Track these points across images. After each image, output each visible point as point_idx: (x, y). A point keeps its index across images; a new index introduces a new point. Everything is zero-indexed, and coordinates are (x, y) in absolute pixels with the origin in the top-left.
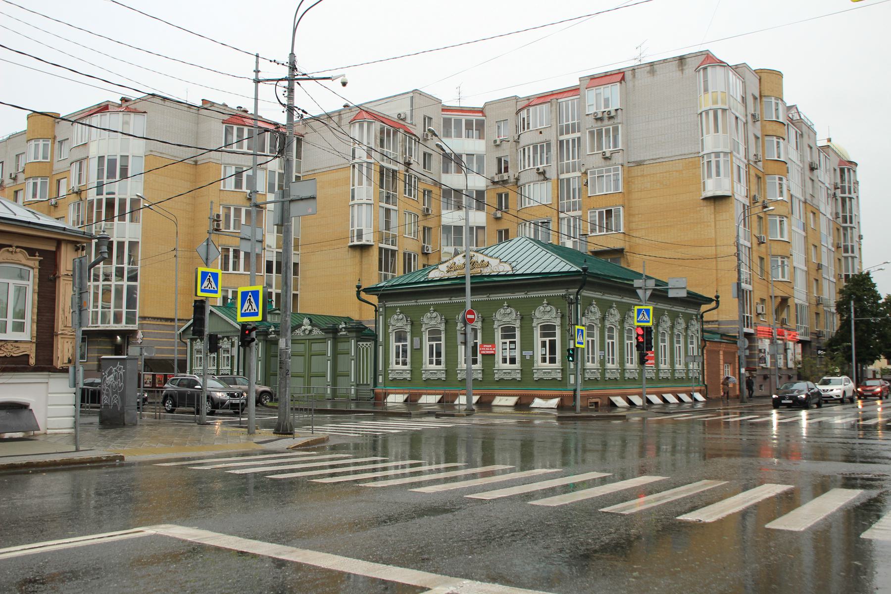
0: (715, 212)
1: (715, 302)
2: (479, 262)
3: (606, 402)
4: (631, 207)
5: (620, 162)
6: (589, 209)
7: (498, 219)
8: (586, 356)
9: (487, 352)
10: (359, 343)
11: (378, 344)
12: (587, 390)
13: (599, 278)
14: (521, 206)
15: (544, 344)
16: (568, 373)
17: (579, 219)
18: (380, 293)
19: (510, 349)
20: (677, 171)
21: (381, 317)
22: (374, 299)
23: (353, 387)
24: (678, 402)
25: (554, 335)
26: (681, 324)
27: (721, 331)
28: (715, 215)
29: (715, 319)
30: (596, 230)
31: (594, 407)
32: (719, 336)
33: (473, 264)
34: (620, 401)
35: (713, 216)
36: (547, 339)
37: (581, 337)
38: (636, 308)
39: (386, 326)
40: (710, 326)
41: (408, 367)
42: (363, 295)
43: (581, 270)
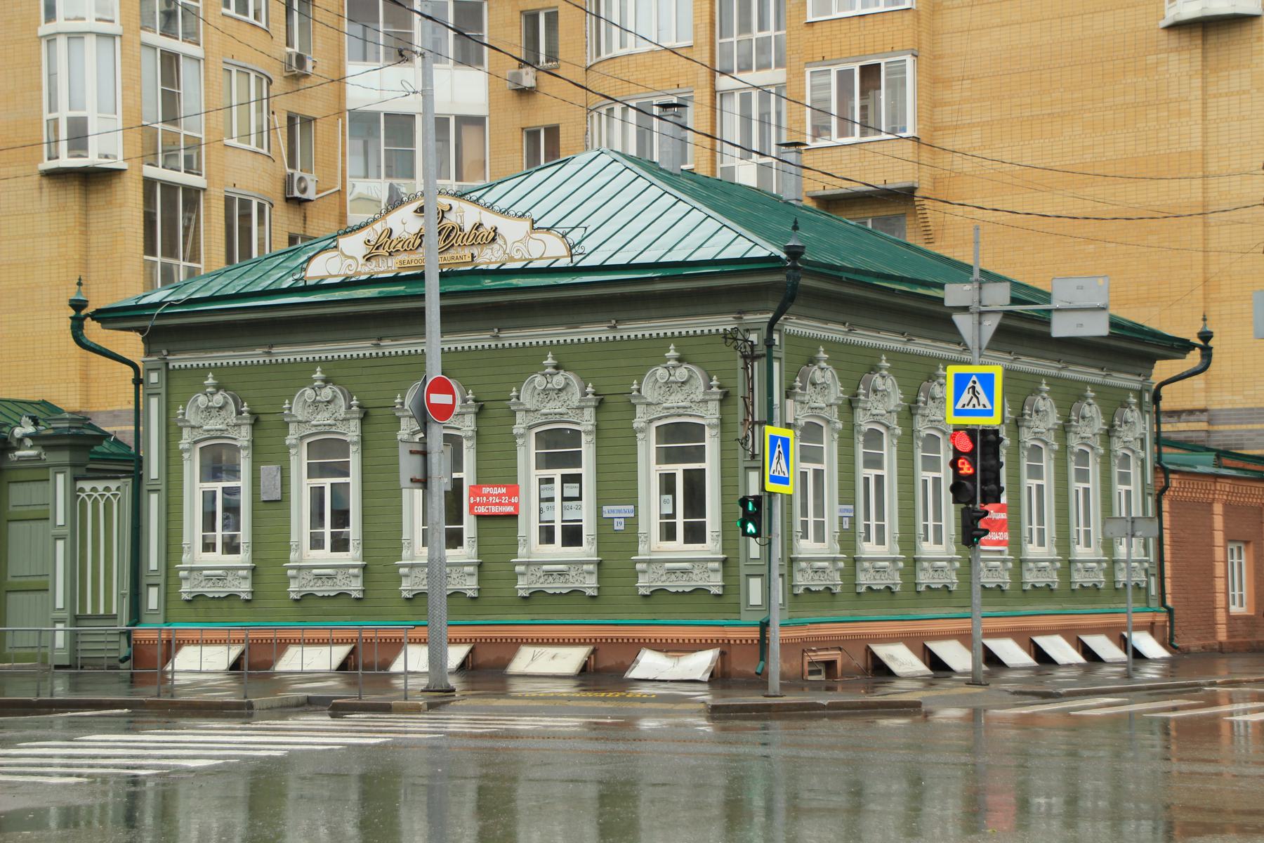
0: (1204, 67)
1: (1197, 350)
2: (467, 229)
3: (859, 661)
4: (941, 57)
6: (808, 64)
7: (524, 93)
8: (798, 519)
9: (495, 510)
10: (80, 484)
11: (145, 488)
12: (804, 624)
13: (838, 280)
14: (598, 54)
15: (668, 484)
16: (744, 571)
17: (778, 95)
18: (149, 324)
19: (564, 499)
21: (154, 402)
22: (130, 344)
23: (60, 626)
24: (1080, 659)
25: (699, 455)
26: (1092, 417)
27: (1216, 442)
28: (1204, 77)
29: (1199, 403)
30: (828, 129)
31: (822, 677)
32: (1211, 457)
33: (449, 235)
34: (902, 659)
35: (1197, 82)
36: (678, 469)
37: (783, 461)
38: (952, 370)
39: (171, 431)
40: (1182, 426)
41: (242, 559)
42: (94, 331)
43: (784, 256)
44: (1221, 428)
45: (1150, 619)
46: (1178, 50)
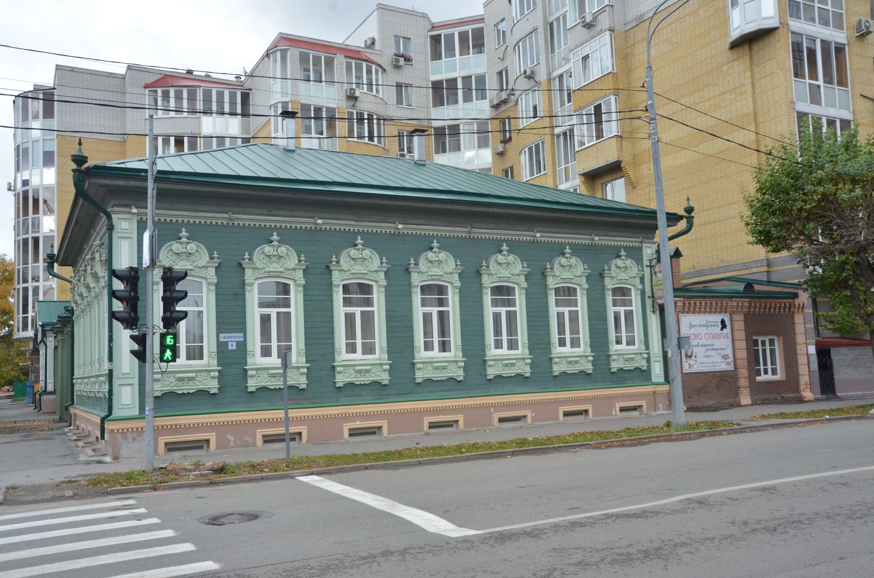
0: (751, 65)
5: (607, 26)
20: (689, 15)
28: (752, 71)
35: (748, 74)
44: (776, 269)
45: (652, 390)
46: (737, 59)
